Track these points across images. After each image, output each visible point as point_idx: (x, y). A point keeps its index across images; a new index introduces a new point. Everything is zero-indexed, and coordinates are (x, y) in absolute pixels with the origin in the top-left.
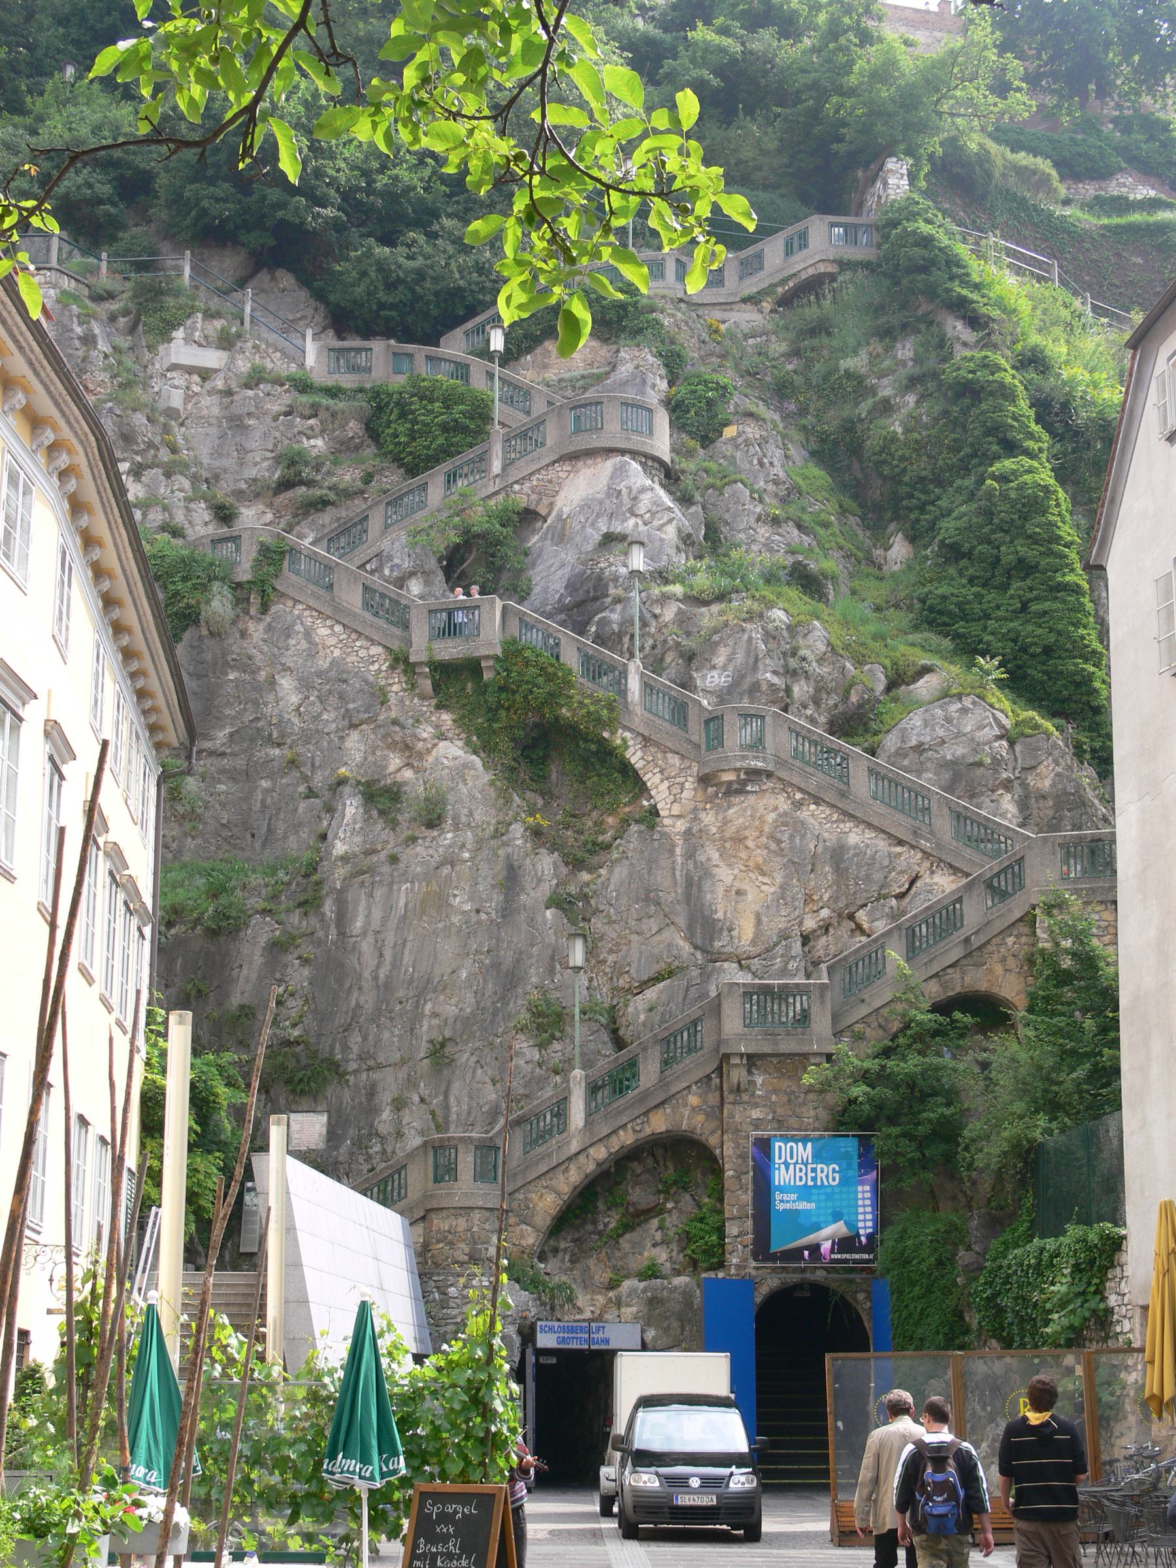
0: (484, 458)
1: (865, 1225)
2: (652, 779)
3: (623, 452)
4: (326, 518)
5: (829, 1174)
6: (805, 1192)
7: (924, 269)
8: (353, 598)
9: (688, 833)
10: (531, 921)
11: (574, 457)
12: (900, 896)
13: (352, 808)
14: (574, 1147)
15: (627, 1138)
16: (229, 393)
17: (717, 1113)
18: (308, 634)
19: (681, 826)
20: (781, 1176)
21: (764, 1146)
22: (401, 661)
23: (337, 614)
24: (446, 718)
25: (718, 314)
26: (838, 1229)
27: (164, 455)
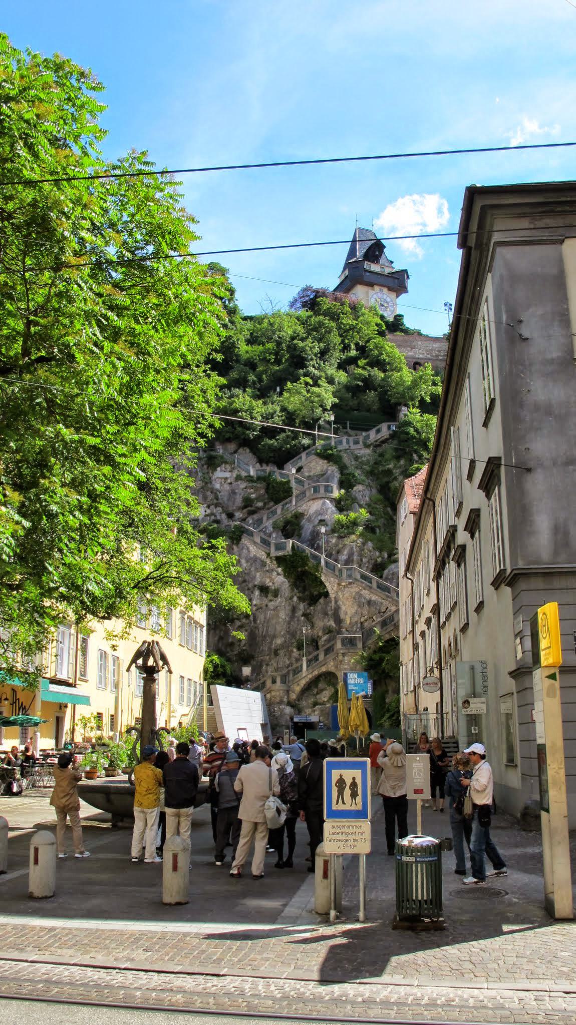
0: (291, 501)
1: (370, 692)
2: (327, 584)
3: (325, 498)
4: (256, 517)
5: (361, 681)
6: (355, 685)
7: (406, 441)
8: (258, 540)
9: (335, 598)
10: (298, 620)
11: (313, 499)
12: (384, 612)
13: (257, 593)
14: (304, 675)
15: (316, 673)
16: (231, 483)
17: (336, 667)
18: (248, 548)
19: (334, 596)
20: (349, 681)
21: (346, 675)
22: (268, 555)
23: (255, 543)
24: (280, 570)
25: (358, 451)
26: (363, 693)
27: (215, 501)
